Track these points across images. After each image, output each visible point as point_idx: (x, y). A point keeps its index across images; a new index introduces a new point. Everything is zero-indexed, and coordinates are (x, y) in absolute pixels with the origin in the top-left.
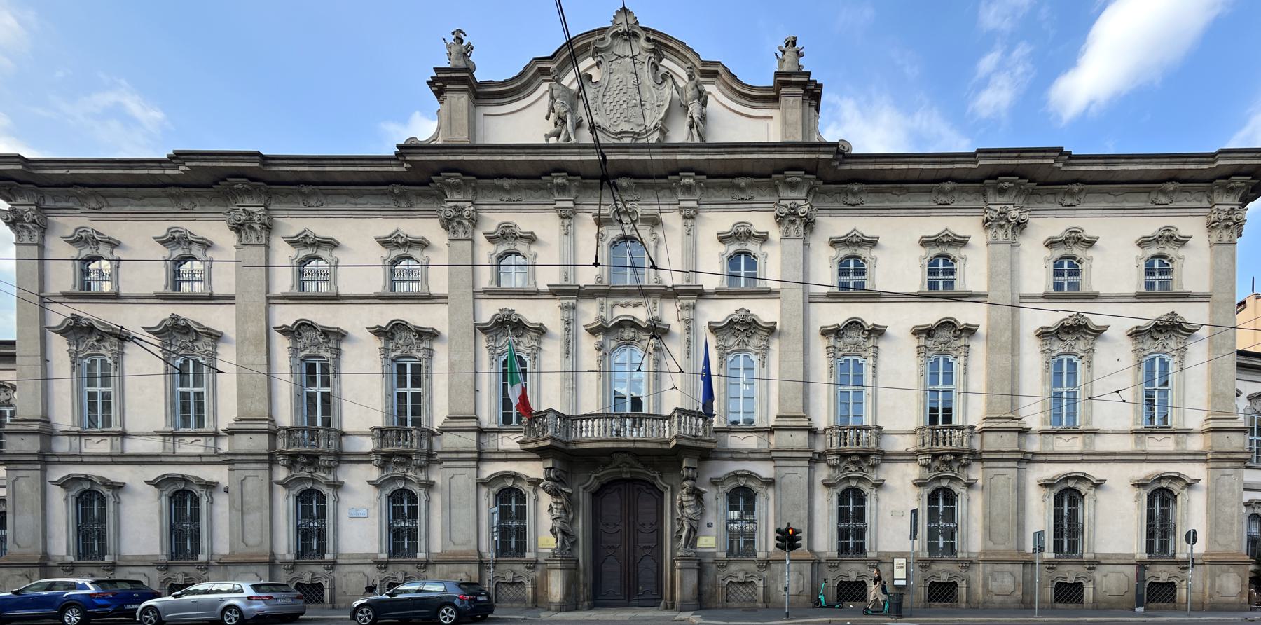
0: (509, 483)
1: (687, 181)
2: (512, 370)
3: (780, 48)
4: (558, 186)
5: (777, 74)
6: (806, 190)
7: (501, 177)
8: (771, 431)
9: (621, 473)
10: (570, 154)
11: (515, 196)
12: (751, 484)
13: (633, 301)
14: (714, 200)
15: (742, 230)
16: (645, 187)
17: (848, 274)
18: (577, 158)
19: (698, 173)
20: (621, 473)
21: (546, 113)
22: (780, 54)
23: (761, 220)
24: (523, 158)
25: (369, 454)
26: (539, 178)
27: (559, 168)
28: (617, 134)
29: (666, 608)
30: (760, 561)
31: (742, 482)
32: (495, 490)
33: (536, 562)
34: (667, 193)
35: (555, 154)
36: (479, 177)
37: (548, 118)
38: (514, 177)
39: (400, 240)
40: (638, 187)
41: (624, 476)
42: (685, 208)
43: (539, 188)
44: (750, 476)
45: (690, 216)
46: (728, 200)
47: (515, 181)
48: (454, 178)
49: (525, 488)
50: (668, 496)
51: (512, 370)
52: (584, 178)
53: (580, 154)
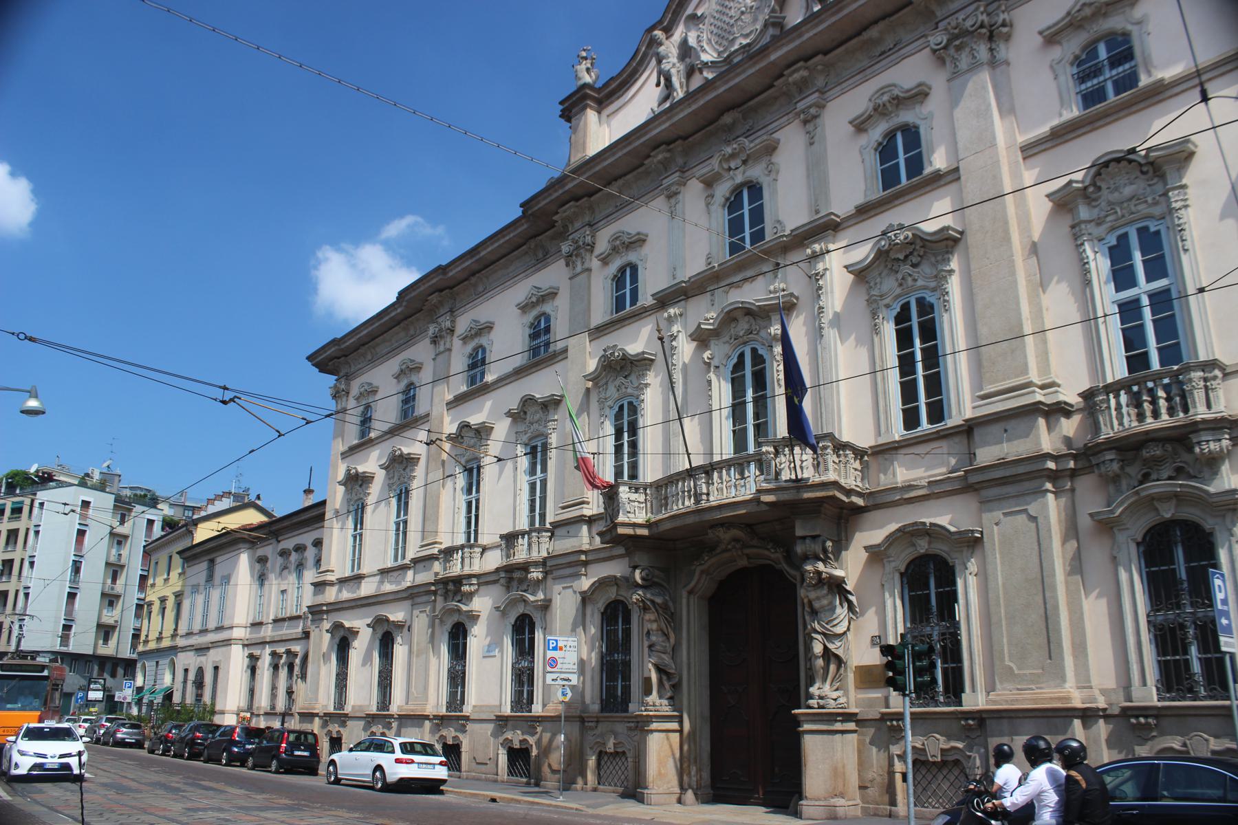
1: (796, 76)
8: (969, 429)
10: (660, 125)
12: (940, 548)
15: (885, 98)
17: (1097, 71)
18: (667, 124)
19: (807, 59)
23: (910, 70)
25: (497, 570)
27: (656, 145)
31: (923, 546)
38: (620, 177)
39: (534, 299)
42: (803, 111)
44: (933, 532)
45: (810, 120)
48: (570, 209)
52: (685, 138)
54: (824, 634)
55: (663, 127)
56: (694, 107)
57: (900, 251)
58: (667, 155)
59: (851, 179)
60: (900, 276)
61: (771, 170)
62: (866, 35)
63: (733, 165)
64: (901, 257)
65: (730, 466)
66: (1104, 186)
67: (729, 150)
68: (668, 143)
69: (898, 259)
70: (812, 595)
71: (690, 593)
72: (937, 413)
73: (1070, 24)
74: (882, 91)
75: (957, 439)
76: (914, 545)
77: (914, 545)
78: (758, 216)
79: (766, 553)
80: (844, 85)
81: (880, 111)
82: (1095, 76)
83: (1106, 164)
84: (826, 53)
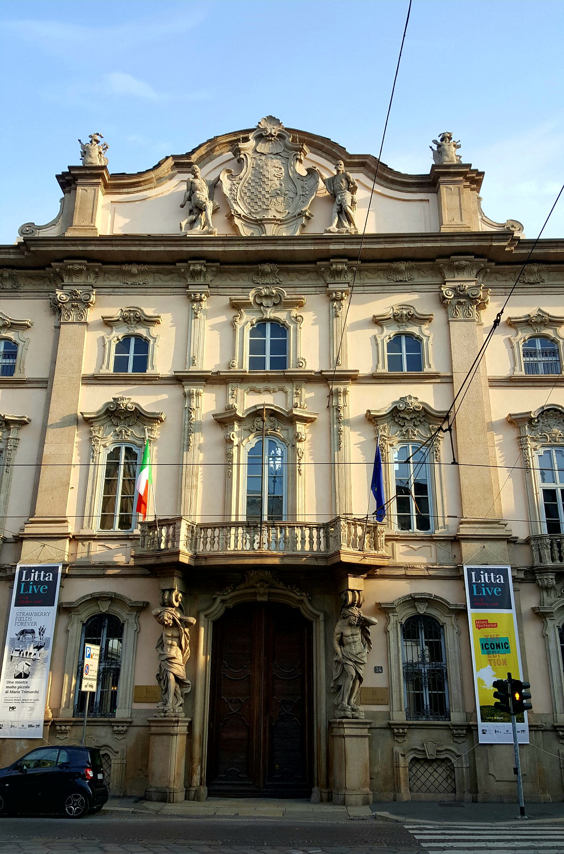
0: (104, 608)
2: (125, 463)
3: (435, 142)
4: (194, 271)
5: (433, 166)
6: (475, 272)
7: (130, 263)
8: (455, 540)
9: (255, 594)
11: (140, 280)
12: (433, 612)
13: (271, 386)
14: (367, 281)
16: (288, 271)
18: (220, 249)
20: (255, 594)
21: (182, 202)
22: (435, 147)
24: (162, 248)
26: (174, 264)
27: (197, 257)
28: (257, 220)
29: (321, 801)
30: (457, 726)
31: (422, 609)
32: (85, 616)
33: (129, 724)
34: (313, 276)
35: (197, 245)
36: (104, 263)
37: (182, 206)
38: (144, 263)
40: (281, 271)
41: (259, 599)
43: (170, 272)
46: (385, 281)
47: (146, 267)
49: (123, 615)
50: (319, 629)
51: (125, 463)
53: (224, 245)
54: (356, 662)
55: (216, 249)
56: (250, 248)
57: (408, 414)
58: (204, 269)
59: (361, 352)
60: (404, 429)
61: (297, 320)
62: (395, 265)
63: (265, 302)
64: (408, 418)
65: (320, 528)
66: (541, 421)
67: (265, 291)
68: (208, 261)
69: (404, 418)
70: (348, 632)
71: (206, 616)
72: (424, 523)
73: (527, 321)
74: (403, 306)
75: (443, 544)
76: (415, 607)
77: (415, 607)
78: (281, 348)
79: (292, 594)
80: (366, 288)
81: (397, 319)
82: (531, 356)
83: (556, 410)
84: (363, 261)
